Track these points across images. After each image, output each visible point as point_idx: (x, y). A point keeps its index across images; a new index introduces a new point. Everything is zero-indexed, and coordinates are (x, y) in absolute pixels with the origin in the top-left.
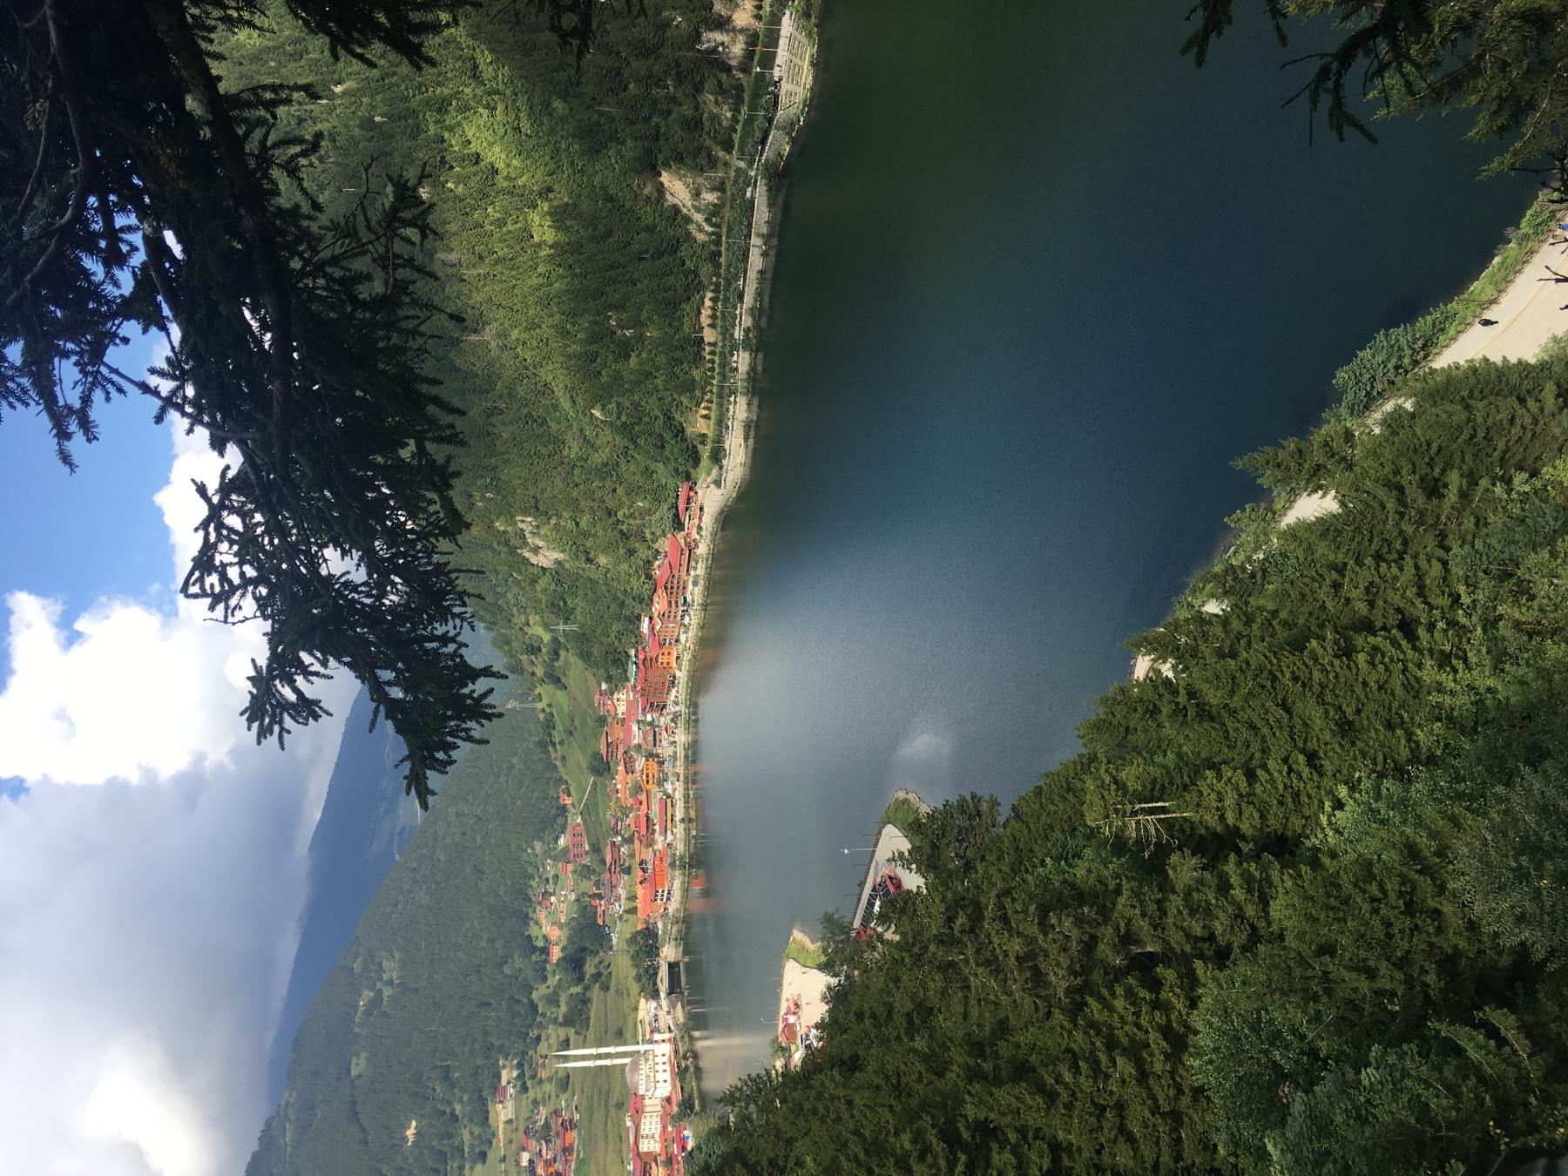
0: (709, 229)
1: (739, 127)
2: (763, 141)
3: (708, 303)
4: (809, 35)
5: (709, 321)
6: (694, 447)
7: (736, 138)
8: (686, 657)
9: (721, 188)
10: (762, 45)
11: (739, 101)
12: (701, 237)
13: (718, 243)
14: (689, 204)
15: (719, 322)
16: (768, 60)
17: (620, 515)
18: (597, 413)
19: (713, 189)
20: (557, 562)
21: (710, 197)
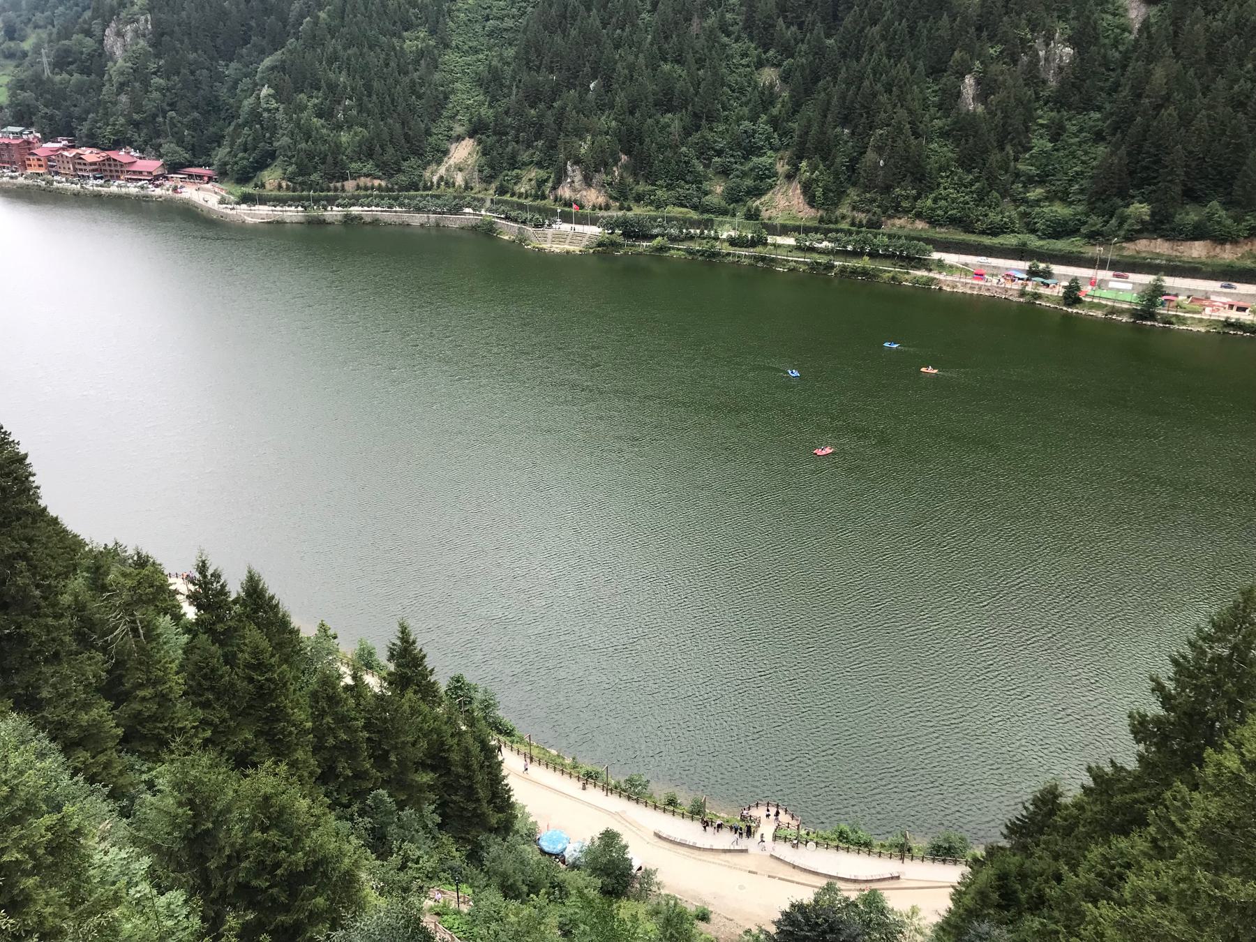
0: (435, 179)
1: (515, 199)
2: (507, 218)
3: (377, 182)
4: (587, 247)
6: (251, 178)
7: (507, 197)
8: (124, 190)
9: (468, 187)
10: (573, 213)
11: (536, 197)
12: (427, 174)
13: (426, 188)
14: (452, 162)
15: (363, 193)
16: (566, 218)
17: (172, 114)
18: (265, 91)
19: (467, 183)
20: (111, 56)
21: (459, 179)
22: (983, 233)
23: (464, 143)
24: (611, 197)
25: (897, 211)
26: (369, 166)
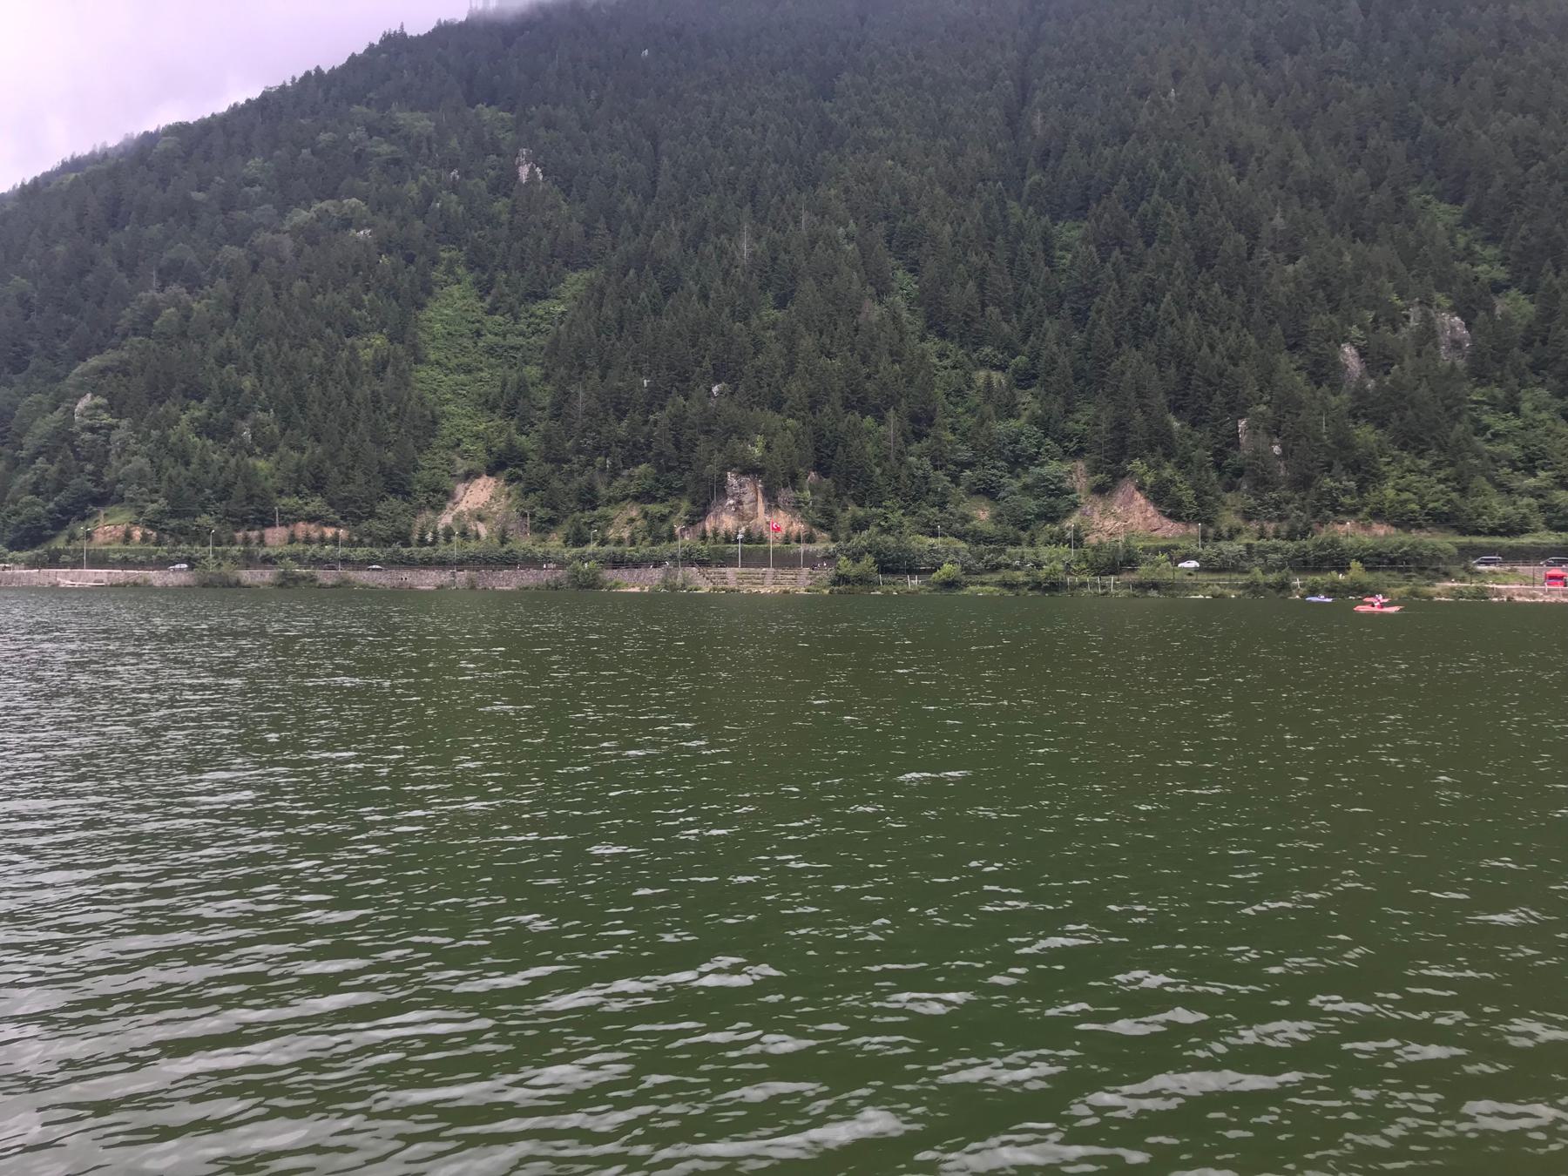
3: (329, 532)
5: (300, 534)
7: (592, 547)
14: (462, 507)
22: (1493, 532)
23: (481, 481)
24: (814, 525)
25: (1336, 512)
26: (316, 504)
